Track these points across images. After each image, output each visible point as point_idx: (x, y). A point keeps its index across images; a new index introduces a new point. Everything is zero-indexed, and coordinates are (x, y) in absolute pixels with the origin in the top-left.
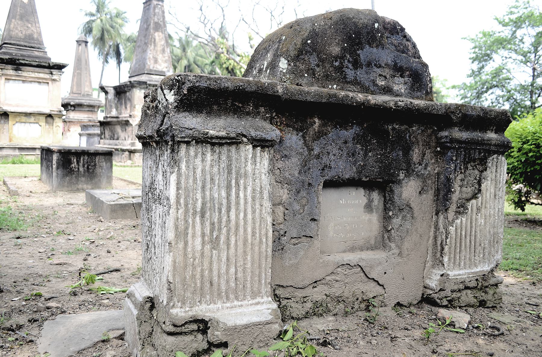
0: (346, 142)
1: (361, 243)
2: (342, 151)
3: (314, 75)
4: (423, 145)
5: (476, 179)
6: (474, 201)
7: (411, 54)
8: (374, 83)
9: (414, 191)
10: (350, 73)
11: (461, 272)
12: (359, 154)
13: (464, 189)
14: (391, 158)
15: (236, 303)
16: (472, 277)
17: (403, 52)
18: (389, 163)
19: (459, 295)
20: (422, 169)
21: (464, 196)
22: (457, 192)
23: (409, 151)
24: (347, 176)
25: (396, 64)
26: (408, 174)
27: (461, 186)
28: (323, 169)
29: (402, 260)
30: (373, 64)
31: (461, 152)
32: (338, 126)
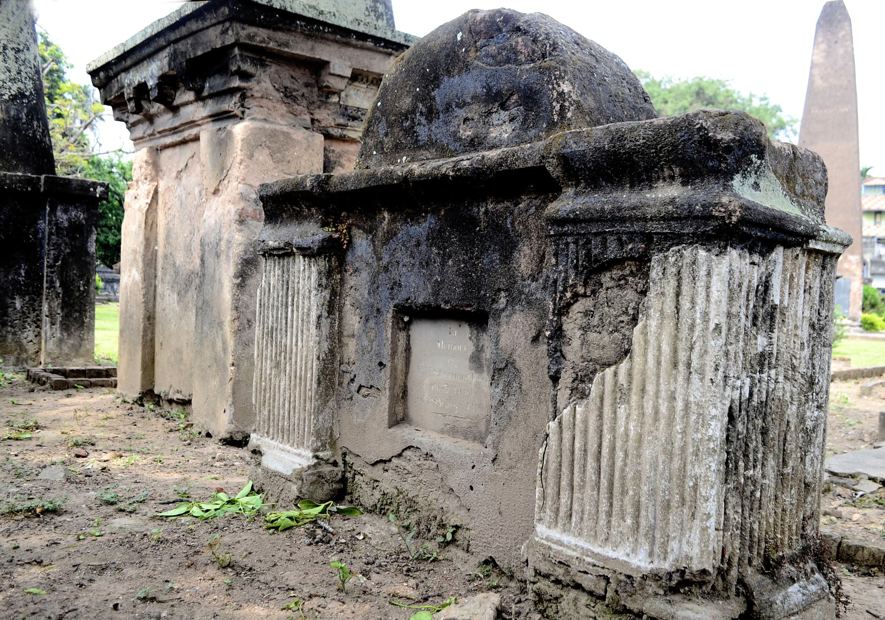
0: (418, 244)
1: (464, 424)
2: (414, 258)
3: (382, 148)
4: (539, 238)
5: (626, 313)
6: (609, 371)
7: (523, 59)
8: (455, 136)
9: (521, 334)
10: (423, 132)
11: (566, 538)
12: (435, 262)
13: (592, 336)
14: (481, 267)
15: (288, 447)
16: (589, 564)
17: (508, 61)
18: (478, 277)
19: (555, 590)
20: (537, 289)
21: (596, 354)
22: (576, 343)
23: (511, 253)
24: (421, 300)
25: (489, 89)
26: (512, 301)
27: (585, 329)
28: (392, 289)
29: (500, 474)
30: (454, 103)
31: (567, 244)
32: (409, 220)
